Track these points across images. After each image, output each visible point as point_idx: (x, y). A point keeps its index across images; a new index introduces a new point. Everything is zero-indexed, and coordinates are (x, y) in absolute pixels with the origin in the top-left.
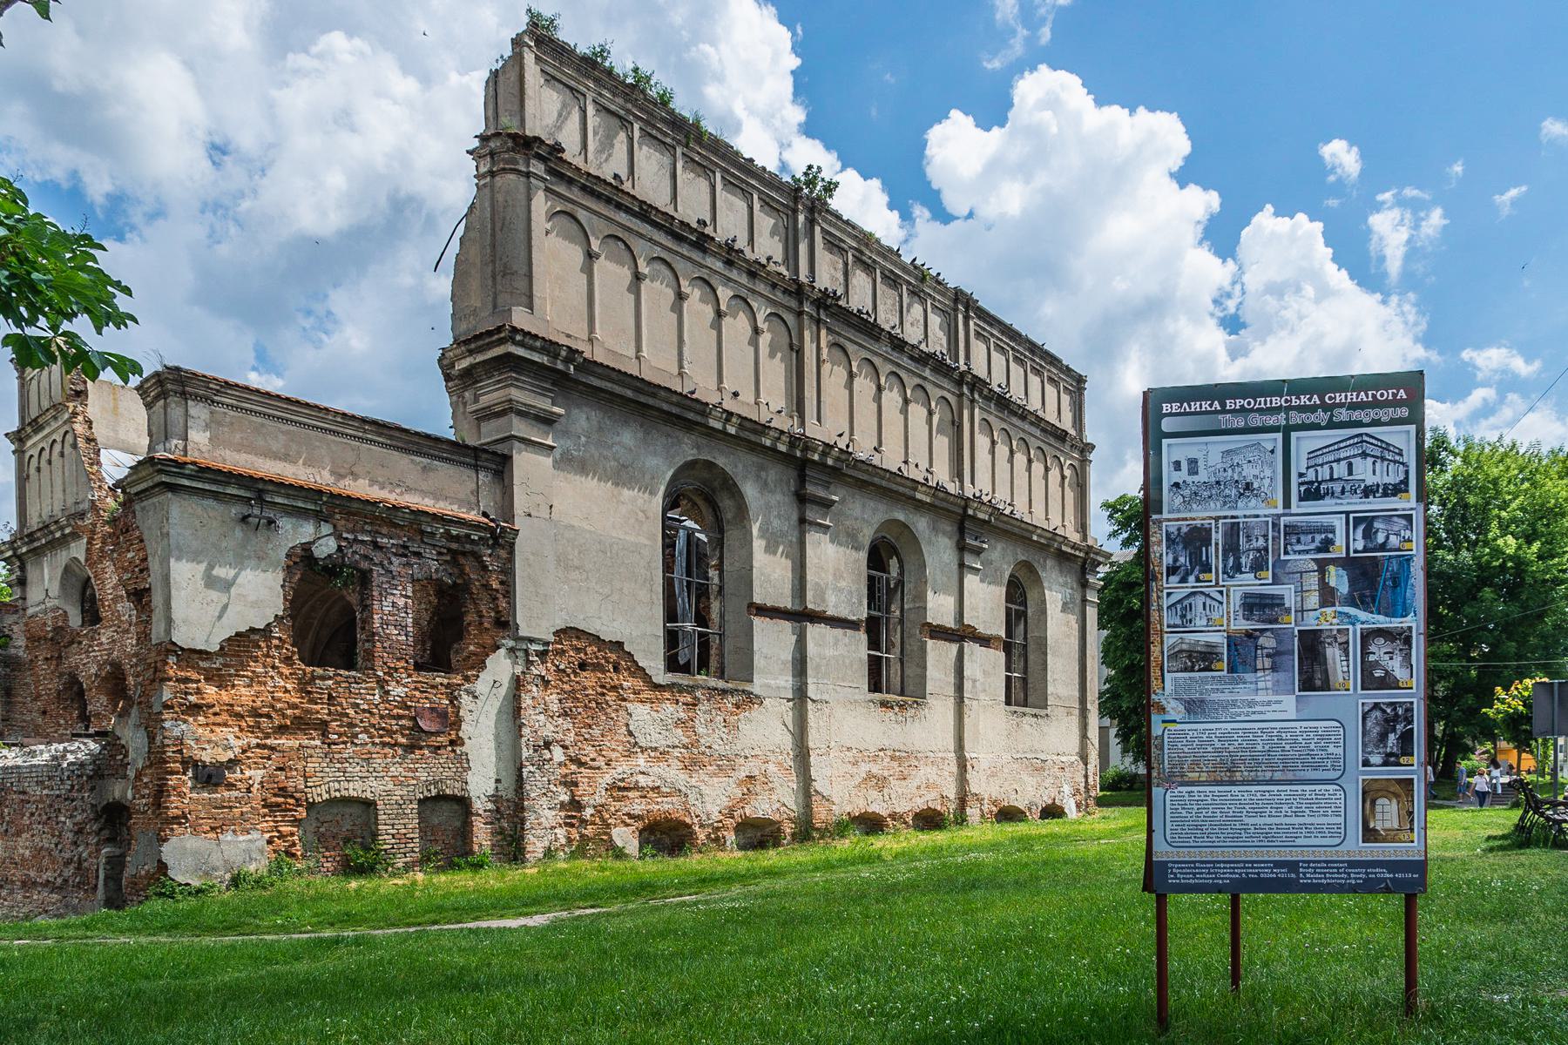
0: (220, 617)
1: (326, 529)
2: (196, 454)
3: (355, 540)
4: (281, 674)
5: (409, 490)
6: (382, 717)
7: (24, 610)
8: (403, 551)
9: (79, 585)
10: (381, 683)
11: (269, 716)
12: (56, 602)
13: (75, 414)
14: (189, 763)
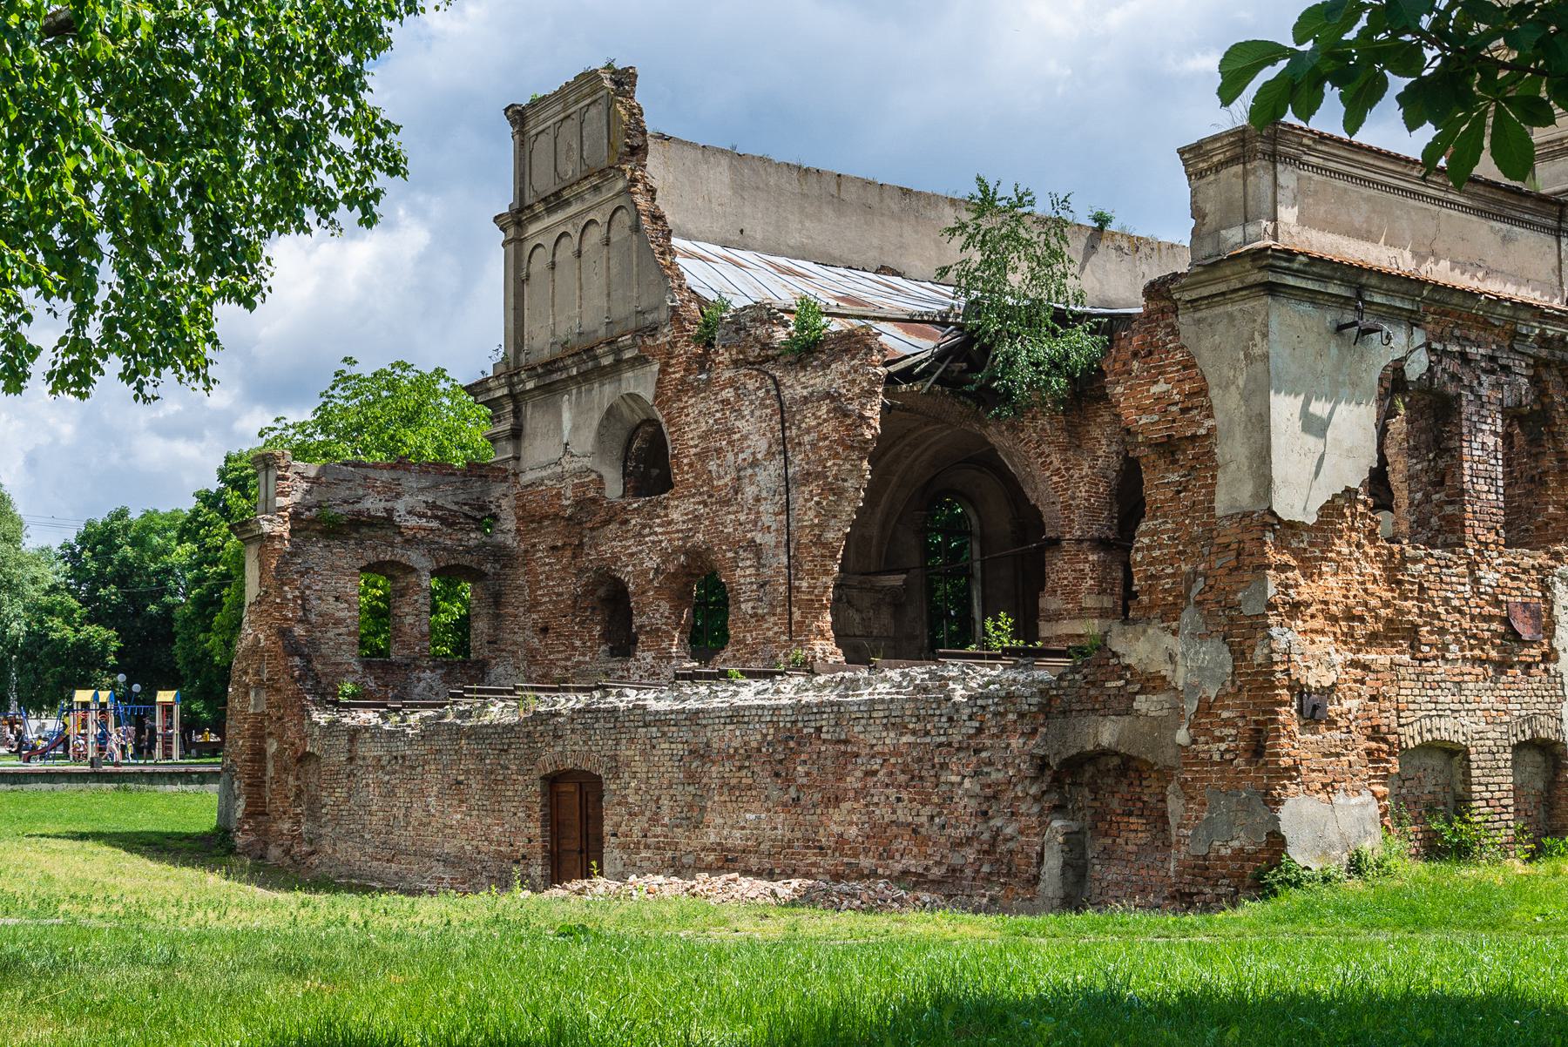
0: (1317, 474)
1: (1419, 337)
2: (1287, 240)
3: (1444, 351)
4: (1365, 554)
5: (1488, 274)
6: (1473, 619)
7: (516, 475)
8: (1495, 366)
9: (623, 435)
10: (1472, 566)
11: (1362, 619)
12: (587, 462)
13: (634, 181)
14: (1298, 689)
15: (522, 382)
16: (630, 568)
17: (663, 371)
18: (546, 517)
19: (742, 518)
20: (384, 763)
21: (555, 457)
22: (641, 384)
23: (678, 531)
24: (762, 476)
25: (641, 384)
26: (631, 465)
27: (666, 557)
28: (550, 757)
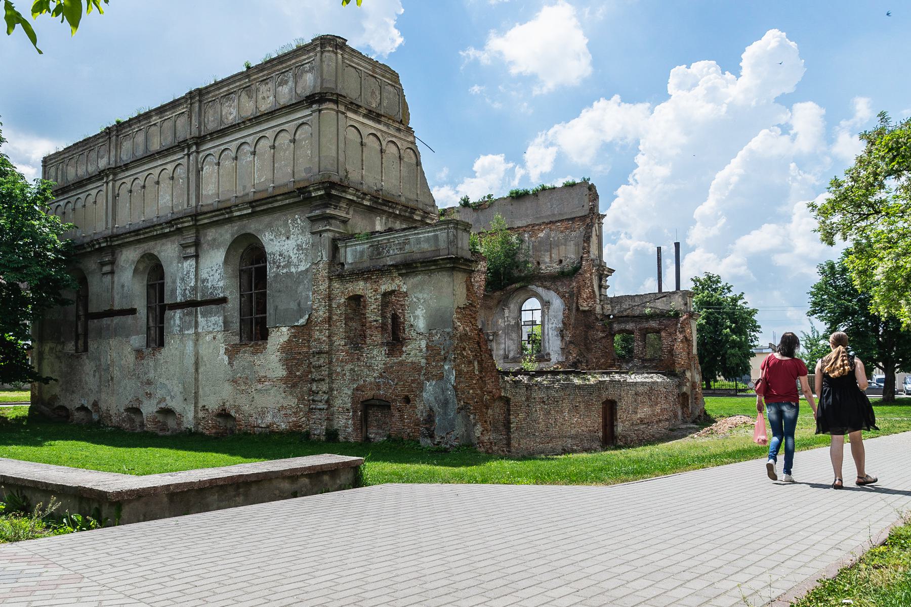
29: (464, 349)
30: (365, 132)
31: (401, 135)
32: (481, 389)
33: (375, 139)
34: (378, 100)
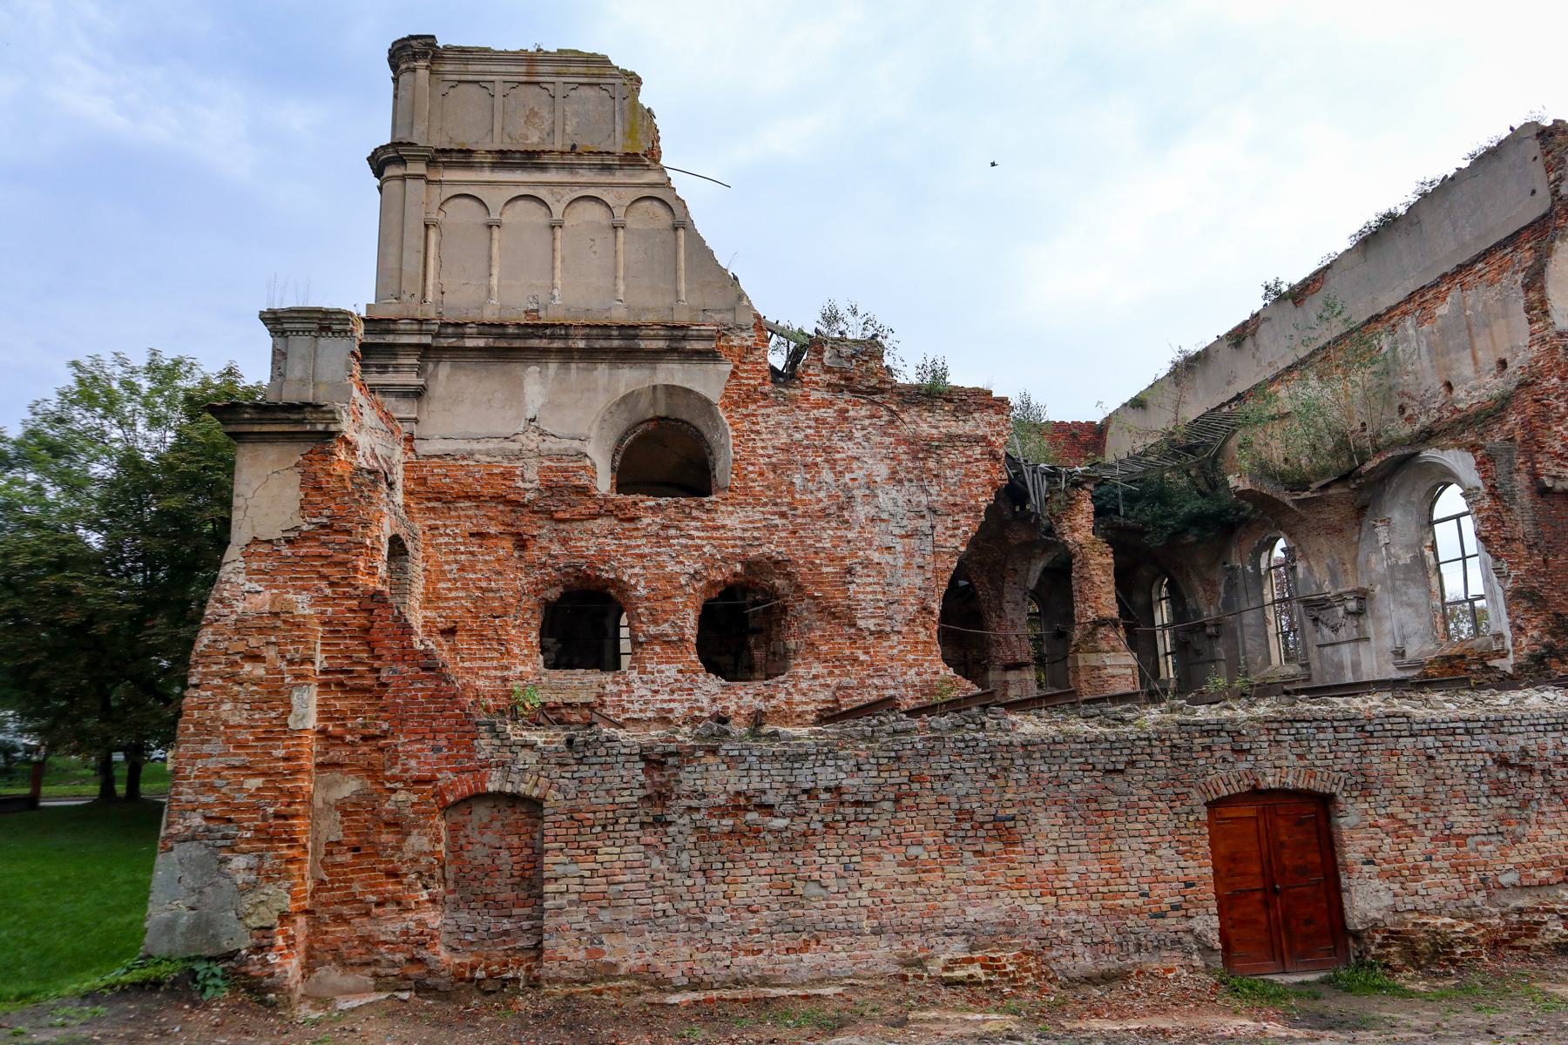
7: (410, 439)
15: (462, 336)
16: (636, 570)
17: (733, 373)
18: (476, 497)
19: (850, 535)
20: (770, 798)
21: (508, 431)
22: (708, 382)
23: (735, 539)
24: (882, 499)
25: (708, 382)
26: (618, 458)
27: (710, 562)
28: (1226, 777)
29: (255, 657)
30: (495, 198)
31: (619, 177)
32: (372, 772)
33: (533, 205)
34: (547, 126)
